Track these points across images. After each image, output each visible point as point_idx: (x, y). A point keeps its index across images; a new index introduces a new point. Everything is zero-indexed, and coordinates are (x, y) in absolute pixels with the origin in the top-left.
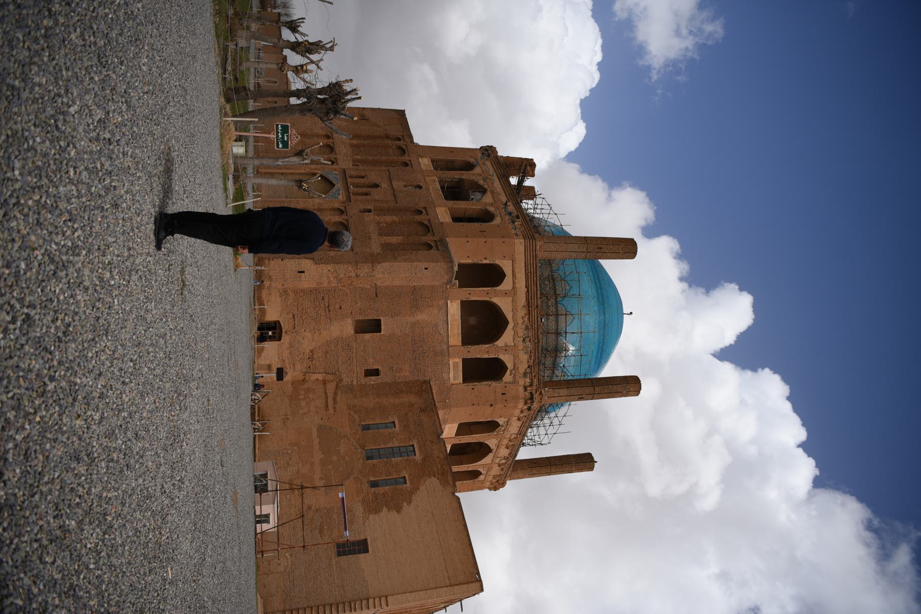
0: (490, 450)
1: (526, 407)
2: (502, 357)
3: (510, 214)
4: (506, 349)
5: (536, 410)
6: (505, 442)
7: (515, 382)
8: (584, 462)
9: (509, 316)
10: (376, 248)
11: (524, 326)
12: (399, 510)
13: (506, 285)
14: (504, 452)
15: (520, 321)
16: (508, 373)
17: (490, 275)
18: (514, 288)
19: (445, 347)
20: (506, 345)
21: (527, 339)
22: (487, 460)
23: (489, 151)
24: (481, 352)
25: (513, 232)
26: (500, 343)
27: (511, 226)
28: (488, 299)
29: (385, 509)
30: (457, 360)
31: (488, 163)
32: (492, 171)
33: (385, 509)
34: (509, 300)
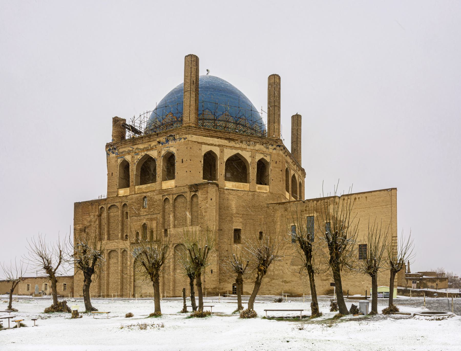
2: (257, 160)
4: (253, 157)
7: (270, 155)
9: (234, 152)
10: (197, 229)
11: (241, 144)
13: (216, 150)
15: (238, 146)
17: (210, 160)
19: (250, 193)
20: (251, 157)
23: (110, 148)
24: (253, 172)
26: (249, 160)
28: (224, 164)
30: (257, 187)
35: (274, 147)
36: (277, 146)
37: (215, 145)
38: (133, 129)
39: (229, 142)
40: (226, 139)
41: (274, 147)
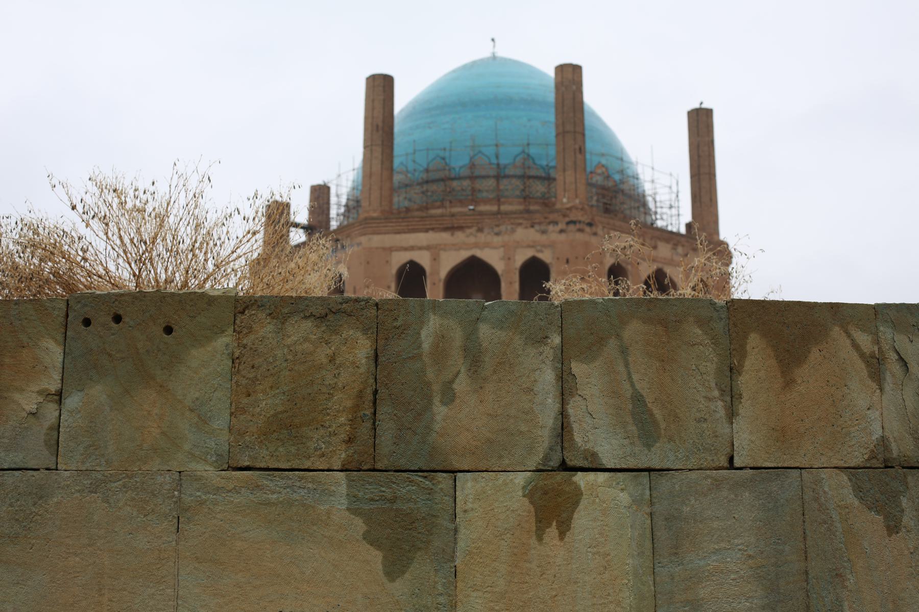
1: (588, 229)
4: (508, 259)
5: (616, 198)
6: (646, 250)
7: (552, 245)
8: (701, 123)
9: (464, 255)
11: (479, 234)
13: (424, 259)
14: (664, 250)
15: (472, 240)
16: (540, 256)
18: (428, 248)
20: (503, 259)
21: (496, 230)
26: (499, 267)
35: (561, 226)
36: (568, 223)
37: (421, 248)
39: (452, 235)
40: (446, 229)
41: (561, 226)
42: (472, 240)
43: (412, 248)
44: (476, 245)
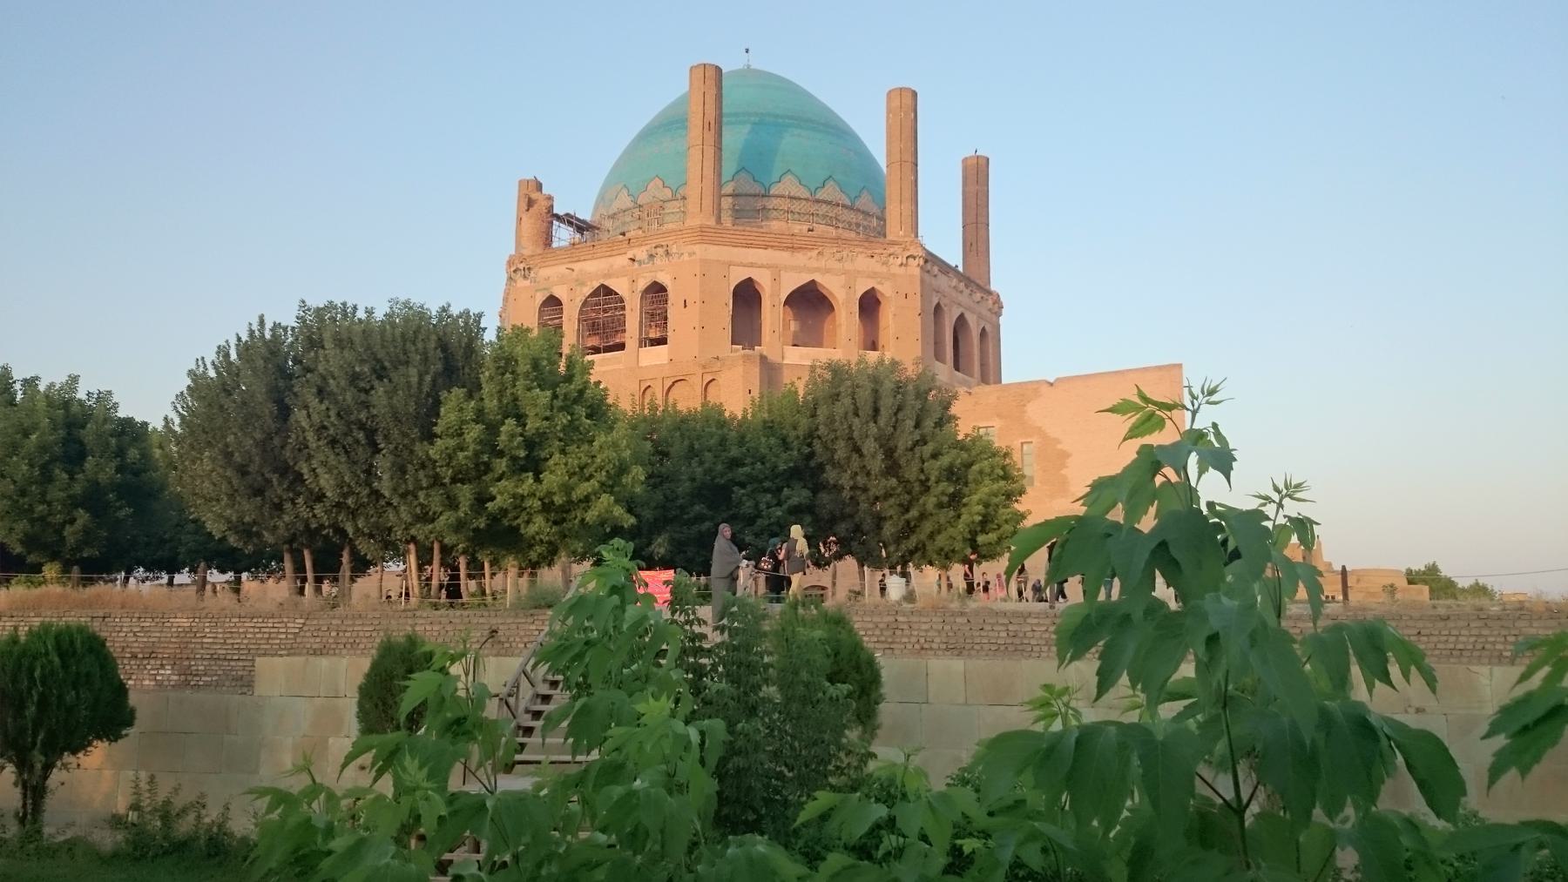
0: (962, 315)
3: (651, 256)
9: (804, 279)
12: (1065, 455)
16: (878, 287)
18: (768, 267)
21: (838, 256)
22: (971, 319)
25: (686, 257)
27: (675, 259)
29: (1063, 472)
31: (544, 272)
32: (562, 269)
33: (1063, 472)
34: (785, 276)
38: (569, 220)
42: (815, 264)
43: (752, 265)
44: (817, 270)
